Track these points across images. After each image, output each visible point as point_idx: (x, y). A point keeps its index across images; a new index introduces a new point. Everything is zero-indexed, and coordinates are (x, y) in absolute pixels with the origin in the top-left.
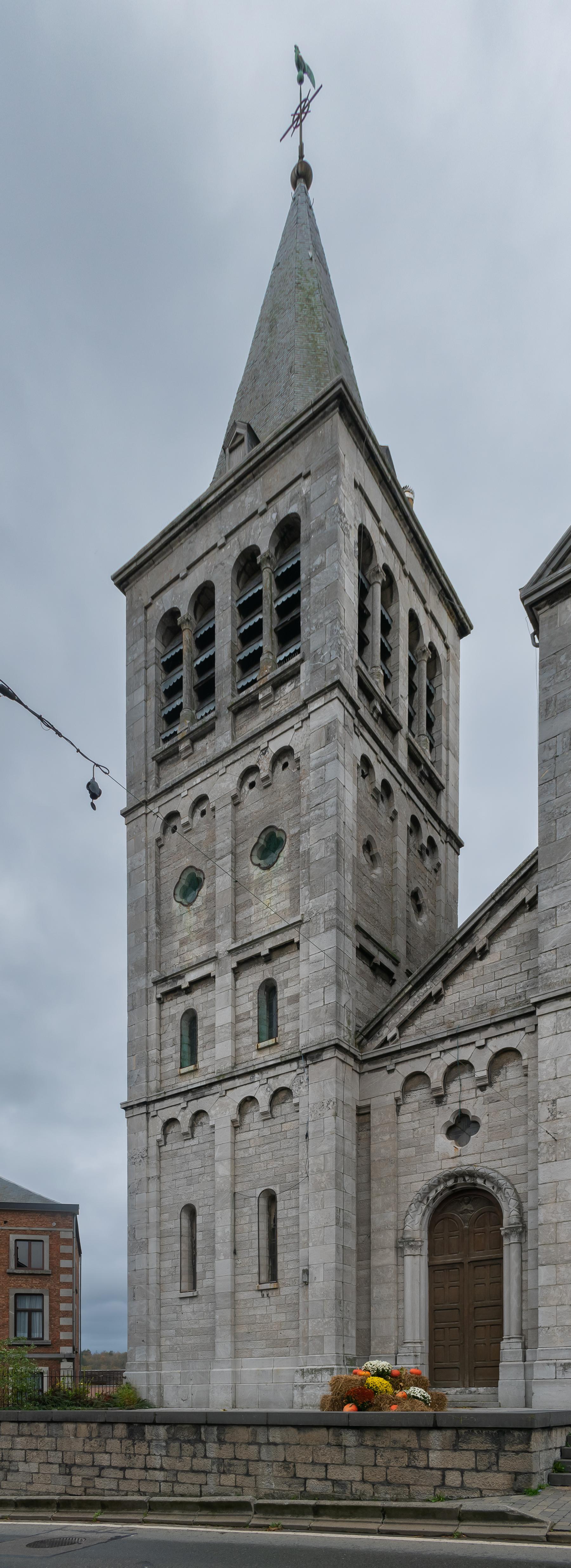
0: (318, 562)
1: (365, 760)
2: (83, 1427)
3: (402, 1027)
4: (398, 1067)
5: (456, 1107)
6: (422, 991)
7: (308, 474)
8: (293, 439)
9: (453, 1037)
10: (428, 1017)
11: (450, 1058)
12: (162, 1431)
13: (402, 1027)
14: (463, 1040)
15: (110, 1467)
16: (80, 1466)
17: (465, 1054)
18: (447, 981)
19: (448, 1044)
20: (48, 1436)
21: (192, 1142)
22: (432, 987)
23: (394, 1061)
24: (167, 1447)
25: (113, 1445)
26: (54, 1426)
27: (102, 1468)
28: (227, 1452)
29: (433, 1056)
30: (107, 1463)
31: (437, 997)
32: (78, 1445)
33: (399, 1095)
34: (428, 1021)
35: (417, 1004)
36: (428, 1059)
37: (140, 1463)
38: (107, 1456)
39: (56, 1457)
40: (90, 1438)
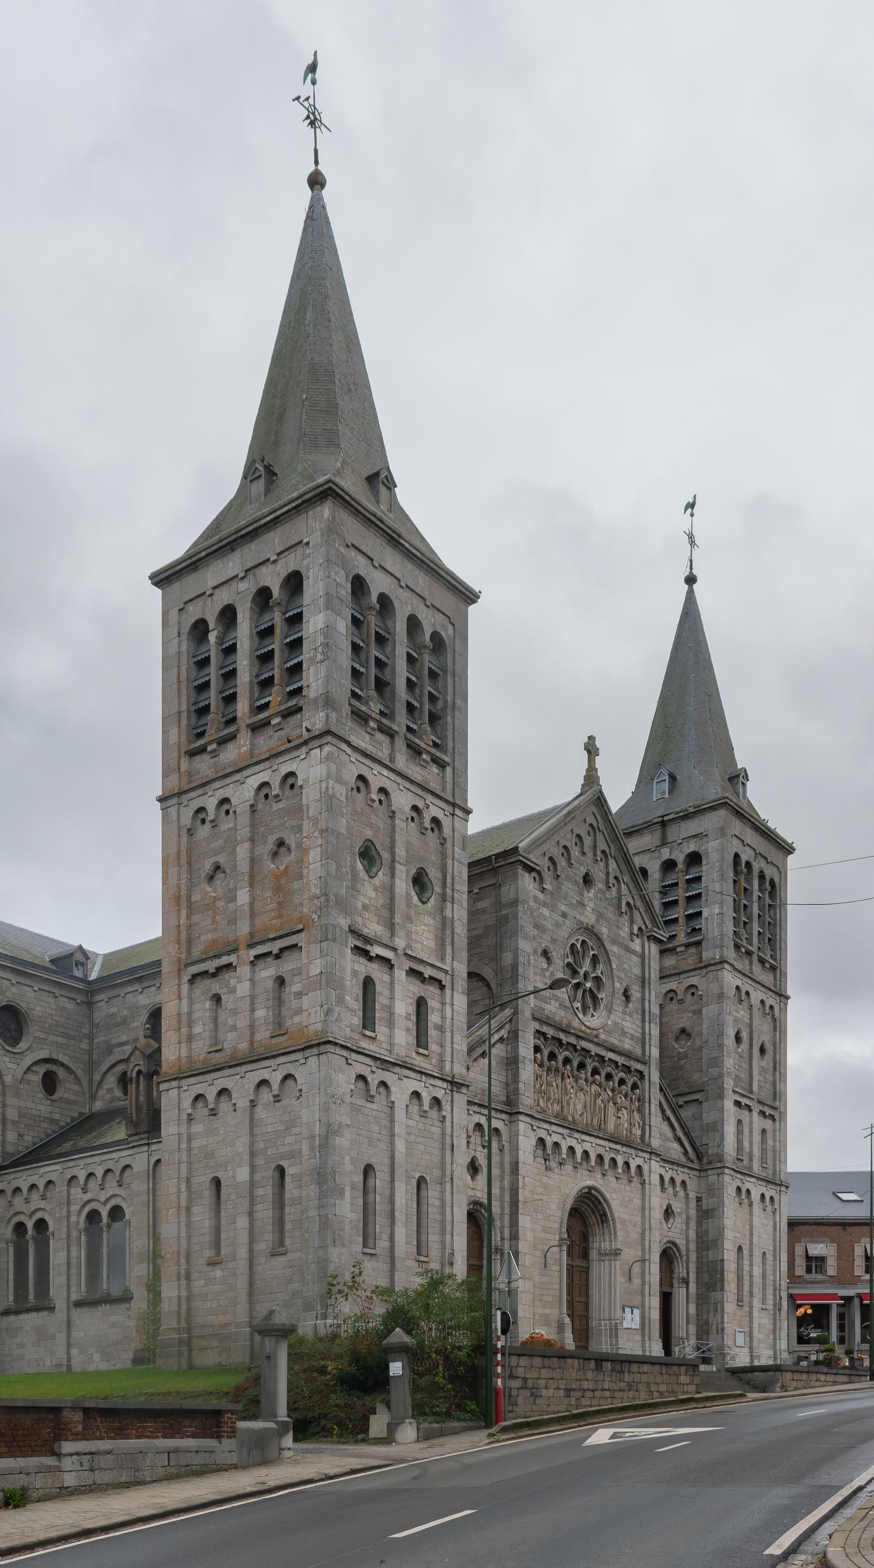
2: (576, 1361)
12: (609, 1364)
15: (588, 1390)
16: (574, 1390)
20: (559, 1368)
24: (611, 1376)
25: (590, 1375)
26: (562, 1360)
27: (584, 1391)
28: (631, 1379)
30: (586, 1387)
32: (574, 1375)
37: (600, 1388)
38: (586, 1382)
39: (562, 1386)
40: (579, 1370)
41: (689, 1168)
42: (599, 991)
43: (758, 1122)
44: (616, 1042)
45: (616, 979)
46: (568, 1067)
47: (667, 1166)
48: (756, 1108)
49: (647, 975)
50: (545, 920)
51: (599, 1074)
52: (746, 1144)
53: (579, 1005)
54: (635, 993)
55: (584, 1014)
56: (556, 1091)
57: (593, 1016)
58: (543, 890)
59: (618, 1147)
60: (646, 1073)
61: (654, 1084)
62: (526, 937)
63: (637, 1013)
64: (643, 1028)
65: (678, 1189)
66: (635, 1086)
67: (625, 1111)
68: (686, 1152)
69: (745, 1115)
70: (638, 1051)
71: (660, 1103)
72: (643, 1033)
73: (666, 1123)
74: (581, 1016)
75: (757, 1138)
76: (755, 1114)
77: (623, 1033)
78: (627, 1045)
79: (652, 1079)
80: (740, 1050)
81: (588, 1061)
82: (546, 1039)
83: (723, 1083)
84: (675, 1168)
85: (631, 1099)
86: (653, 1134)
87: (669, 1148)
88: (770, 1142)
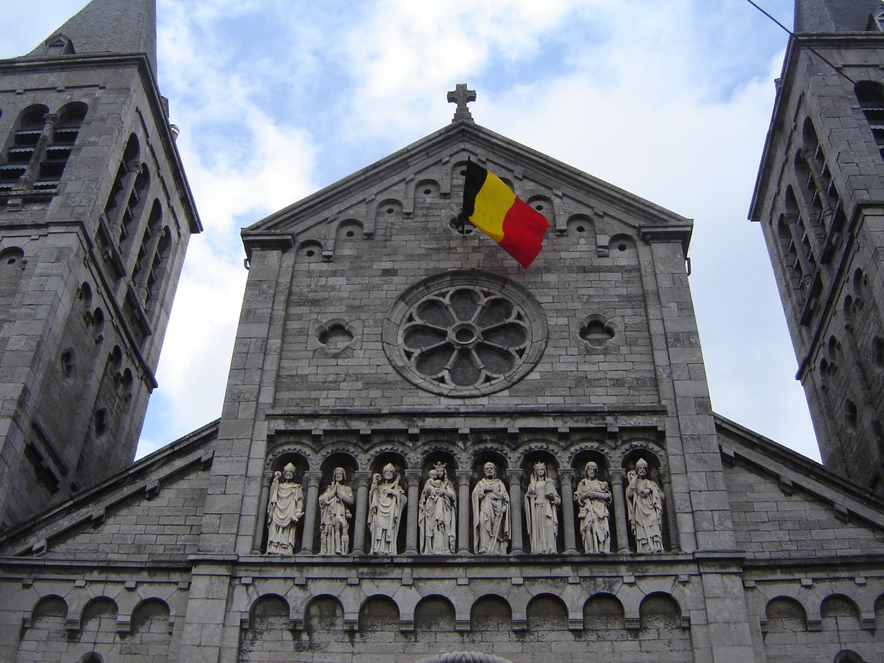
0: (93, 139)
1: (86, 287)
5: (89, 648)
6: (83, 511)
7: (104, 88)
8: (100, 64)
9: (102, 569)
11: (97, 591)
19: (95, 576)
22: (95, 510)
31: (97, 523)
70: (645, 399)
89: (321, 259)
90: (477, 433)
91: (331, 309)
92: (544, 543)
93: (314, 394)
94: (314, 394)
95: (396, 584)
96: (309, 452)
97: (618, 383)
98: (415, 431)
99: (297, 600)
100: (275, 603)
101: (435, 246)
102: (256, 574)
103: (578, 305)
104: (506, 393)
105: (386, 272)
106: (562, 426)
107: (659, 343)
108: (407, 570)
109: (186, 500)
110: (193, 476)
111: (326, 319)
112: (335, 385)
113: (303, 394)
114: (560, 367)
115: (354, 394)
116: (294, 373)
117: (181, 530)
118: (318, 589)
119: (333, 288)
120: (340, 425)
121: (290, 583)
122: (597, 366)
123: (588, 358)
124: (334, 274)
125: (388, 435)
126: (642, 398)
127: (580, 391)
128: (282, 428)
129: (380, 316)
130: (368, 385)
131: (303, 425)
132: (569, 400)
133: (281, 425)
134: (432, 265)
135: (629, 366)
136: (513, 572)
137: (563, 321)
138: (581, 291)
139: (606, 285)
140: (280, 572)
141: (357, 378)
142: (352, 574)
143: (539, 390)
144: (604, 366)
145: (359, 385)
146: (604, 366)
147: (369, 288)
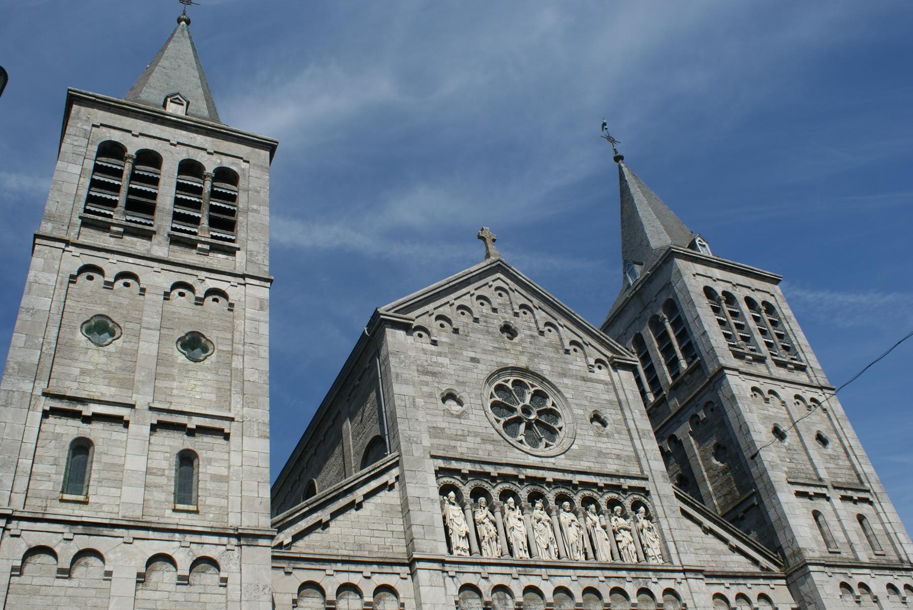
3: (297, 537)
4: (295, 572)
6: (315, 515)
10: (315, 537)
11: (343, 578)
13: (297, 537)
14: (353, 567)
17: (355, 579)
18: (334, 515)
19: (339, 566)
21: (66, 582)
22: (323, 515)
23: (292, 565)
29: (328, 572)
31: (324, 525)
33: (296, 597)
34: (316, 541)
35: (310, 524)
36: (322, 573)
41: (764, 578)
42: (556, 422)
43: (848, 511)
44: (591, 464)
45: (573, 406)
46: (511, 500)
47: (727, 582)
48: (835, 495)
49: (622, 397)
50: (443, 366)
51: (571, 500)
52: (838, 535)
53: (523, 438)
54: (610, 415)
55: (535, 445)
56: (491, 526)
57: (547, 445)
58: (434, 343)
59: (623, 573)
60: (648, 485)
61: (667, 497)
62: (406, 382)
63: (619, 433)
64: (634, 446)
65: (755, 606)
66: (636, 506)
67: (626, 534)
68: (756, 562)
69: (821, 505)
70: (635, 470)
71: (684, 513)
72: (635, 450)
73: (710, 536)
74: (527, 448)
75: (853, 526)
76: (837, 502)
77: (600, 453)
78: (611, 467)
79: (662, 493)
80: (786, 444)
81: (545, 490)
82: (464, 477)
83: (769, 478)
84: (741, 581)
85: (635, 518)
86: (681, 549)
87: (726, 562)
88: (876, 527)
89: (429, 341)
90: (557, 483)
91: (445, 381)
92: (604, 556)
93: (453, 443)
94: (453, 443)
95: (539, 578)
96: (460, 485)
97: (618, 457)
98: (522, 477)
99: (485, 587)
100: (469, 588)
101: (496, 345)
102: (457, 570)
103: (586, 403)
104: (563, 456)
105: (473, 360)
106: (601, 481)
107: (635, 435)
108: (543, 570)
109: (383, 512)
110: (382, 494)
111: (444, 388)
112: (462, 438)
113: (446, 442)
114: (588, 443)
115: (477, 446)
116: (435, 425)
117: (385, 534)
118: (497, 580)
119: (442, 365)
120: (478, 468)
121: (478, 576)
122: (605, 445)
123: (600, 439)
124: (440, 354)
125: (505, 478)
126: (632, 468)
127: (600, 460)
128: (443, 466)
129: (478, 392)
130: (484, 441)
131: (454, 465)
132: (597, 465)
133: (441, 463)
134: (499, 359)
135: (620, 447)
136: (598, 573)
137: (581, 412)
138: (586, 394)
139: (597, 391)
140: (471, 568)
141: (476, 435)
142: (514, 570)
143: (578, 457)
144: (609, 445)
145: (478, 440)
146: (609, 445)
147: (465, 369)
